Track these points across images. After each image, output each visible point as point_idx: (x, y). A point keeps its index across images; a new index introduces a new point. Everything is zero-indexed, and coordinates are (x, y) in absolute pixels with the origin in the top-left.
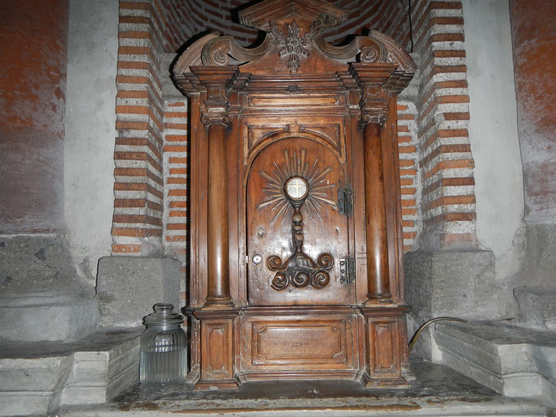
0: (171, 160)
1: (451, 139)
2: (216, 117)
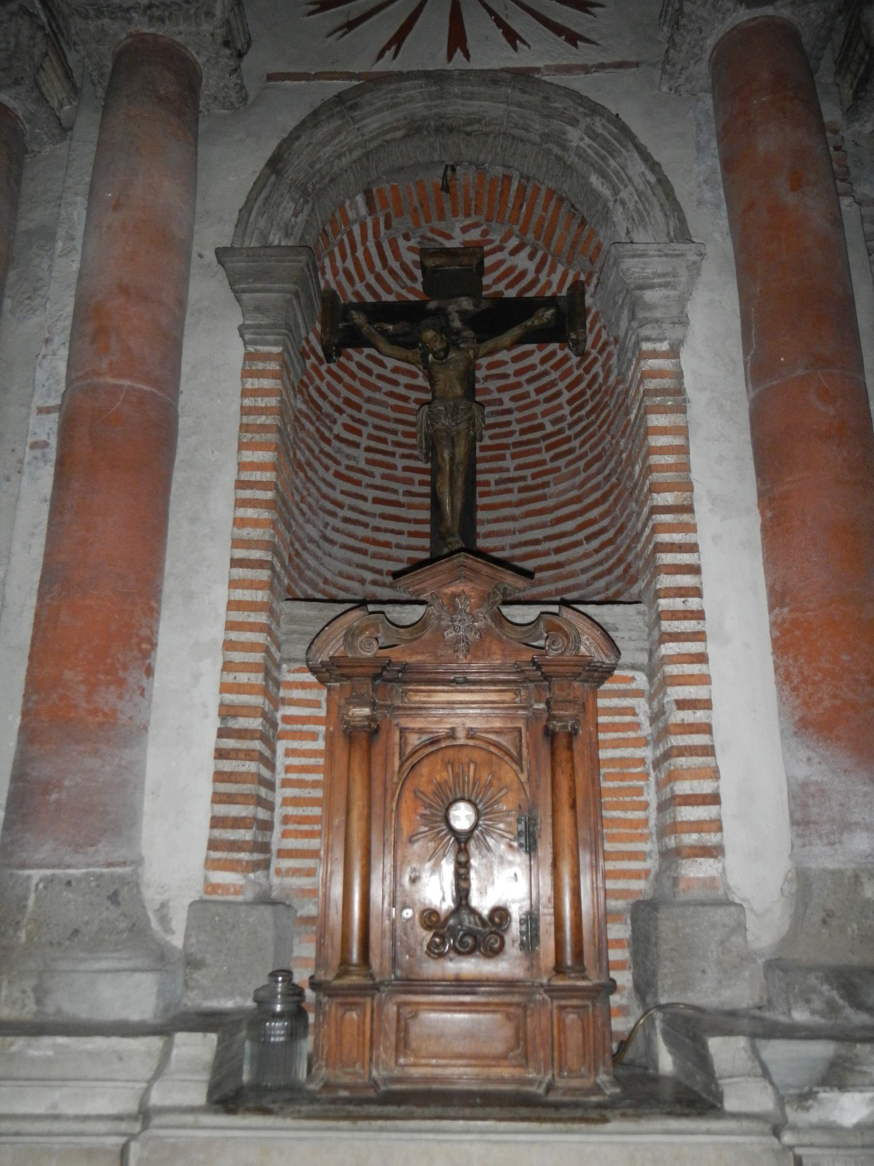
0: (289, 753)
1: (686, 737)
2: (360, 721)
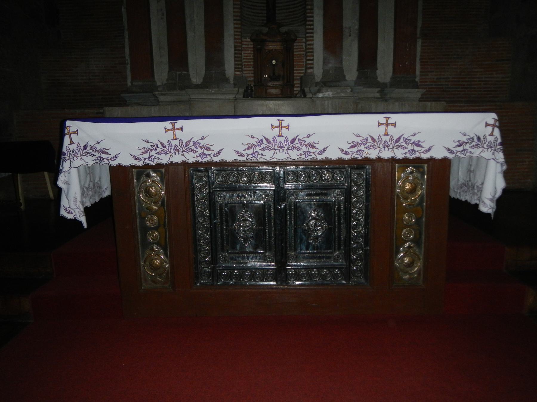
0: (244, 54)
